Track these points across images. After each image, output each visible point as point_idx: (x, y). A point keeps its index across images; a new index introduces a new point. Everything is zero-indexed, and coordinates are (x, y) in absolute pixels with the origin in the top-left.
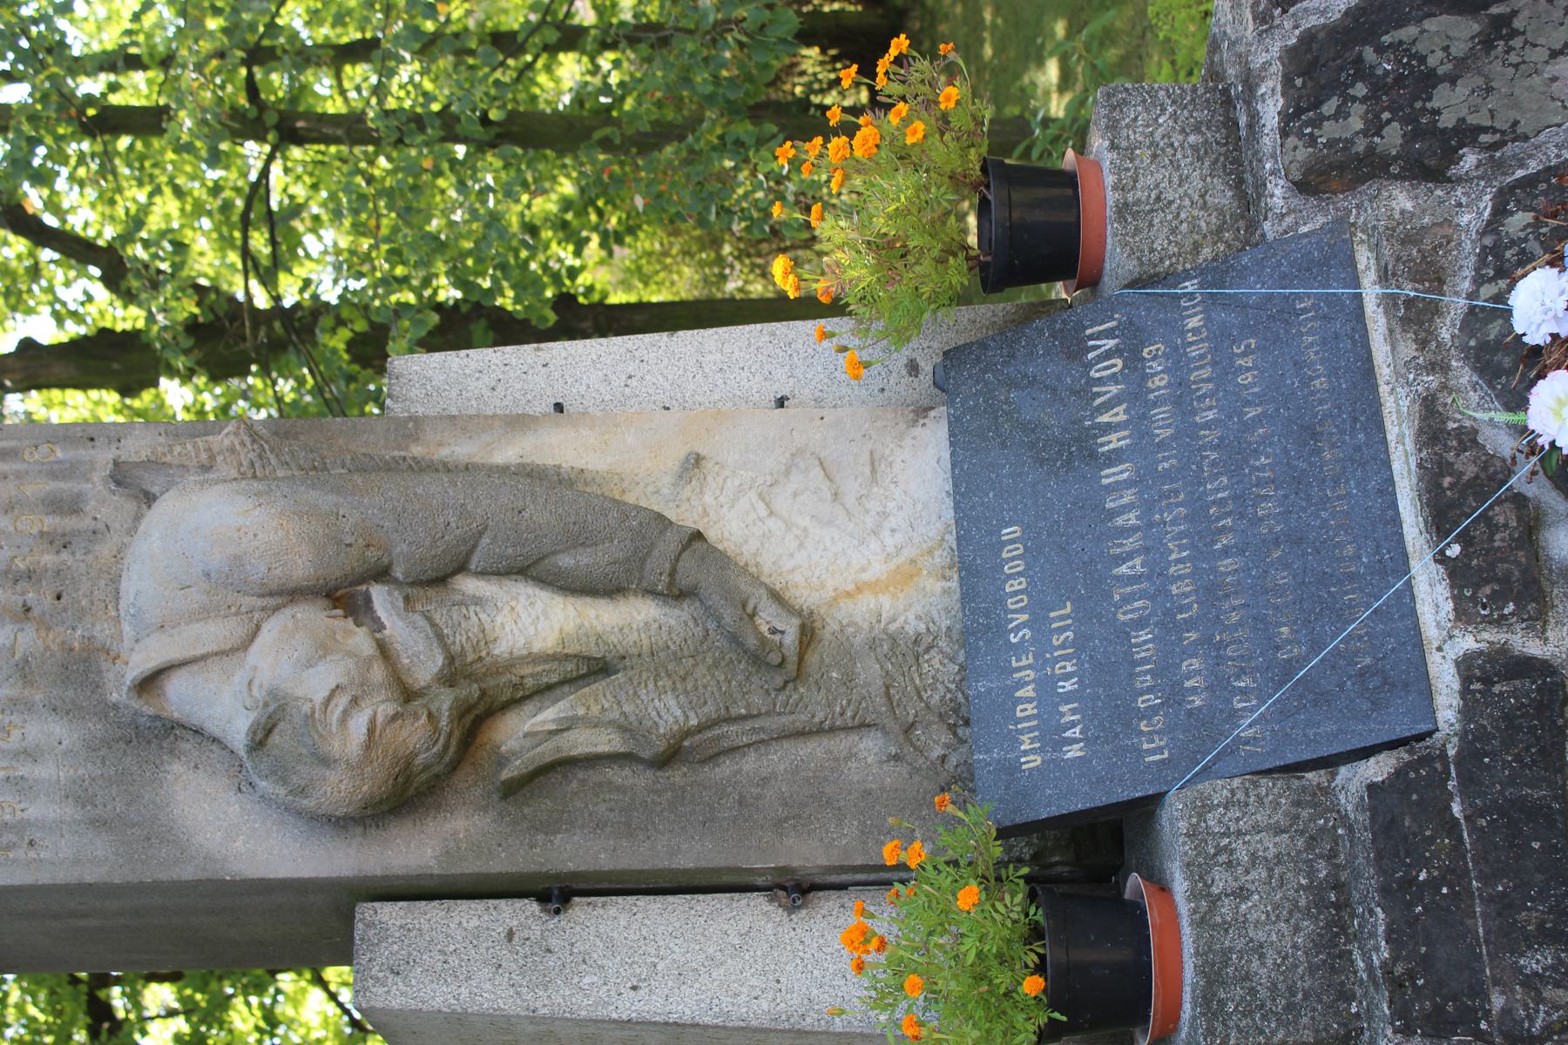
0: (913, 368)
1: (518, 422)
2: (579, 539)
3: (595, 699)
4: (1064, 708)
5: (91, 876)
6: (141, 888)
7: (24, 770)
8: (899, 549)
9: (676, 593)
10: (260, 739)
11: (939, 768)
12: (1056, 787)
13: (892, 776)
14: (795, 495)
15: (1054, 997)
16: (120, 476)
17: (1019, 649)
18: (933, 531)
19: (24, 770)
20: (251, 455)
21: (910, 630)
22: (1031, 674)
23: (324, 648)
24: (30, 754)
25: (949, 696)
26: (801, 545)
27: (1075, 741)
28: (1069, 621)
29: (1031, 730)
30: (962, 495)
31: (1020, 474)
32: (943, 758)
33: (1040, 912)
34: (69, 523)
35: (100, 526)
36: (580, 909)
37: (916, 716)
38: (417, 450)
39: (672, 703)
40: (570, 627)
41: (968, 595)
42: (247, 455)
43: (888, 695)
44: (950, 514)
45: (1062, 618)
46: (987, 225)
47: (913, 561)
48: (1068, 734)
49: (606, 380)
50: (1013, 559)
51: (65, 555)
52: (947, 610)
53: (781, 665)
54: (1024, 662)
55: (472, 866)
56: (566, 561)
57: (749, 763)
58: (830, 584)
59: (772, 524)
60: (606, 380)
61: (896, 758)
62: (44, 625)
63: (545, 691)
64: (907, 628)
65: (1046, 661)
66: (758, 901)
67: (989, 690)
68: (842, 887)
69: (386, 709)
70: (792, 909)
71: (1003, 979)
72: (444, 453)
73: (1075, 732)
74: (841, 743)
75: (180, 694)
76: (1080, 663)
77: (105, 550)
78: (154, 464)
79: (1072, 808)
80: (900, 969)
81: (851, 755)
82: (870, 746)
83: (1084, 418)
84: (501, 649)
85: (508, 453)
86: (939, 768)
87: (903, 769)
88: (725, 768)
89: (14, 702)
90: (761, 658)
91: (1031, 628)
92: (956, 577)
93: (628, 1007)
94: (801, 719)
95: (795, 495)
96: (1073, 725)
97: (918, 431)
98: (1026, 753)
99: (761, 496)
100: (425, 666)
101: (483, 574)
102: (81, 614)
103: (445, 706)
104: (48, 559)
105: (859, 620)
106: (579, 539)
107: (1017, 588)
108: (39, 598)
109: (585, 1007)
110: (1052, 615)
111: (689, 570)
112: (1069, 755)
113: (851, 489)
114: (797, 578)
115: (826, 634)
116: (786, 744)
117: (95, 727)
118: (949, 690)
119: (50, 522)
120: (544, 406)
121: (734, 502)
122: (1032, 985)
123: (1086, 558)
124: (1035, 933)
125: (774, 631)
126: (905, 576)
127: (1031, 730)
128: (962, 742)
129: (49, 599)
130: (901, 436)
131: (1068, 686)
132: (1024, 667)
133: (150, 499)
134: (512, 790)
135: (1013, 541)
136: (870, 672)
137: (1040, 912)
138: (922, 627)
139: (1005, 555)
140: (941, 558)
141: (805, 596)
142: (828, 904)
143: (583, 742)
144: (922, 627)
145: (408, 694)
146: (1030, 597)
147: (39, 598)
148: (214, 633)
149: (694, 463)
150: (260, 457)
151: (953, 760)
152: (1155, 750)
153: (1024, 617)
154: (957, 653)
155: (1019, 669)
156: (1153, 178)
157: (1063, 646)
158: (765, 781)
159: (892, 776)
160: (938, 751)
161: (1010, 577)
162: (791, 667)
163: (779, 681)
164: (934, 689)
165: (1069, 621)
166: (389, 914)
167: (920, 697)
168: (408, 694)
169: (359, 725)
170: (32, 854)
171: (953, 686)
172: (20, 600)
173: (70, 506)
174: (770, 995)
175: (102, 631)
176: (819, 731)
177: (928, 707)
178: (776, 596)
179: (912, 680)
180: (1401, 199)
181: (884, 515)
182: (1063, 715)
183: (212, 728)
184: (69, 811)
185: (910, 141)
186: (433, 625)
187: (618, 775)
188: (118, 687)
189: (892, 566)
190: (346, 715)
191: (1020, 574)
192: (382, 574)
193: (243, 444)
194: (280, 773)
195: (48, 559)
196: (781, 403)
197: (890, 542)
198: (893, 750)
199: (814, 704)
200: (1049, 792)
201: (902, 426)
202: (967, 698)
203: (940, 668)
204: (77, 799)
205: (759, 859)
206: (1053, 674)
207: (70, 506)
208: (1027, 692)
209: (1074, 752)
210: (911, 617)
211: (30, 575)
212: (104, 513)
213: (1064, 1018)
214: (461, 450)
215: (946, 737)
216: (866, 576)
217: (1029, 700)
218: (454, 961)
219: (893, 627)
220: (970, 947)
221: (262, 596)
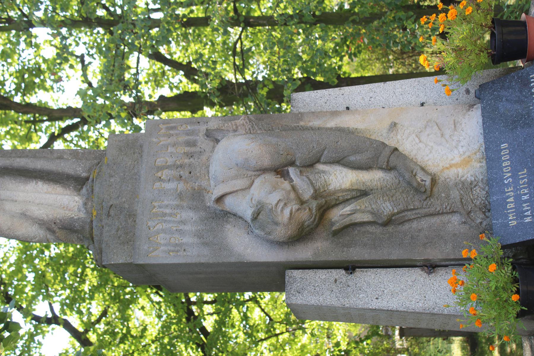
0: (468, 92)
1: (335, 113)
2: (357, 151)
3: (363, 203)
4: (524, 205)
5: (203, 260)
6: (218, 265)
7: (181, 227)
8: (464, 153)
9: (389, 168)
10: (255, 217)
11: (480, 226)
12: (522, 232)
13: (463, 229)
14: (428, 135)
15: (522, 302)
16: (208, 134)
17: (508, 185)
18: (476, 147)
19: (181, 227)
20: (249, 126)
21: (469, 180)
22: (512, 194)
23: (275, 188)
24: (183, 222)
25: (482, 202)
26: (431, 152)
27: (528, 216)
28: (526, 176)
29: (512, 212)
30: (487, 133)
31: (507, 126)
32: (481, 223)
33: (517, 273)
34: (193, 149)
35: (202, 150)
36: (359, 273)
37: (471, 208)
38: (302, 123)
39: (388, 205)
40: (354, 180)
41: (489, 168)
42: (248, 126)
43: (461, 201)
44: (482, 140)
45: (523, 174)
46: (494, 41)
47: (469, 157)
48: (526, 214)
49: (363, 98)
50: (505, 155)
51: (192, 160)
52: (482, 173)
53: (425, 192)
54: (510, 190)
55: (323, 258)
56: (352, 158)
57: (415, 224)
58: (441, 165)
59: (421, 145)
60: (363, 98)
61: (465, 223)
62: (186, 182)
63: (346, 201)
64: (468, 179)
65: (517, 189)
66: (418, 270)
67: (497, 199)
68: (446, 266)
69: (295, 207)
70: (429, 273)
71: (505, 296)
72: (311, 124)
73: (529, 213)
74: (445, 218)
75: (230, 203)
76: (530, 190)
77: (204, 158)
78: (219, 130)
79: (528, 239)
80: (468, 292)
81: (449, 222)
82: (455, 219)
83: (530, 106)
84: (331, 187)
85: (332, 124)
86: (480, 226)
87: (467, 227)
88: (407, 226)
89: (178, 206)
90: (418, 190)
91: (512, 178)
92: (484, 162)
93: (375, 304)
94: (432, 210)
95: (428, 135)
96: (528, 210)
97: (470, 113)
98: (511, 220)
99: (417, 136)
100: (307, 193)
101: (325, 163)
103: (314, 206)
104: (187, 161)
105: (451, 177)
106: (357, 151)
107: (507, 164)
109: (360, 304)
110: (520, 173)
111: (394, 161)
112: (526, 221)
113: (447, 133)
114: (430, 163)
115: (440, 181)
116: (427, 218)
117: (203, 214)
118: (482, 200)
119: (187, 149)
120: (342, 108)
121: (408, 138)
122: (515, 298)
123: (531, 154)
124: (515, 281)
125: (422, 181)
126: (467, 162)
127: (512, 212)
128: (488, 217)
129: (187, 174)
130: (464, 115)
131: (526, 197)
132: (510, 192)
133: (217, 141)
134: (336, 233)
135: (505, 149)
136: (455, 194)
137: (517, 273)
138: (473, 179)
139: (502, 154)
140: (479, 155)
141: (432, 169)
142: (441, 272)
143: (359, 218)
144: (473, 179)
145: (302, 203)
146: (511, 167)
147: (185, 173)
148: (240, 183)
149: (394, 125)
150: (252, 127)
151: (484, 223)
153: (510, 174)
154: (485, 187)
155: (508, 192)
157: (524, 184)
158: (420, 230)
159: (463, 229)
160: (479, 221)
161: (504, 161)
162: (428, 192)
163: (424, 197)
164: (478, 200)
165: (526, 176)
166: (297, 273)
167: (473, 202)
168: (302, 203)
169: (287, 212)
170: (185, 253)
171: (484, 199)
172: (179, 174)
173: (193, 144)
174: (422, 302)
175: (204, 184)
176: (438, 214)
177: (475, 205)
178: (423, 169)
179: (470, 196)
181: (459, 141)
182: (524, 207)
183: (240, 214)
184: (196, 240)
185: (467, 13)
186: (310, 180)
187: (371, 229)
188: (210, 200)
189: (462, 158)
190: (282, 211)
191: (508, 160)
192: (292, 164)
193: (246, 123)
194: (262, 228)
195: (187, 161)
196: (422, 105)
197: (461, 150)
198: (464, 220)
199: (436, 205)
200: (519, 233)
201: (465, 111)
202: (489, 203)
203: (479, 193)
204: (198, 236)
205: (418, 256)
206: (520, 193)
207: (193, 144)
208: (511, 200)
209: (528, 220)
210: (469, 175)
211: (181, 166)
213: (526, 309)
214: (316, 123)
215: (482, 216)
216: (453, 162)
217: (512, 202)
218: (317, 288)
219: (463, 179)
220: (493, 285)
221: (255, 171)
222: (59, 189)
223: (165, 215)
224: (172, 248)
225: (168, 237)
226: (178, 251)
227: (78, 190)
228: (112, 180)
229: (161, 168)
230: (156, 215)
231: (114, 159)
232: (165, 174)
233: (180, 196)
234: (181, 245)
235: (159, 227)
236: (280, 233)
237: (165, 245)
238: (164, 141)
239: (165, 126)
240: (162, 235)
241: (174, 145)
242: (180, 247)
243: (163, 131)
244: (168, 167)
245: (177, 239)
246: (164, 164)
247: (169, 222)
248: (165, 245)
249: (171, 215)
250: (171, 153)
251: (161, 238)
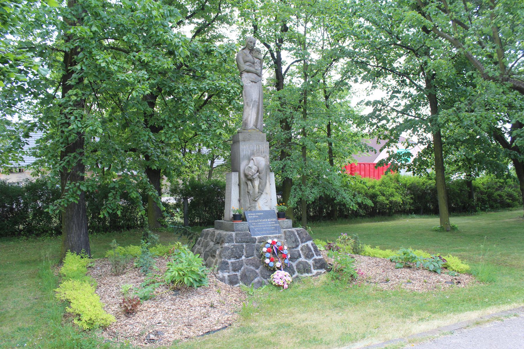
1: (269, 182)
10: (250, 167)
75: (252, 161)
82: (249, 205)
85: (267, 181)
93: (232, 189)
100: (254, 177)
106: (262, 186)
126: (260, 207)
134: (246, 183)
143: (249, 187)
148: (256, 163)
152: (250, 221)
156: (286, 223)
180: (283, 237)
214: (268, 178)
222: (255, 121)
227: (254, 125)
232: (258, 147)
236: (247, 172)
245: (245, 150)
251: (245, 147)
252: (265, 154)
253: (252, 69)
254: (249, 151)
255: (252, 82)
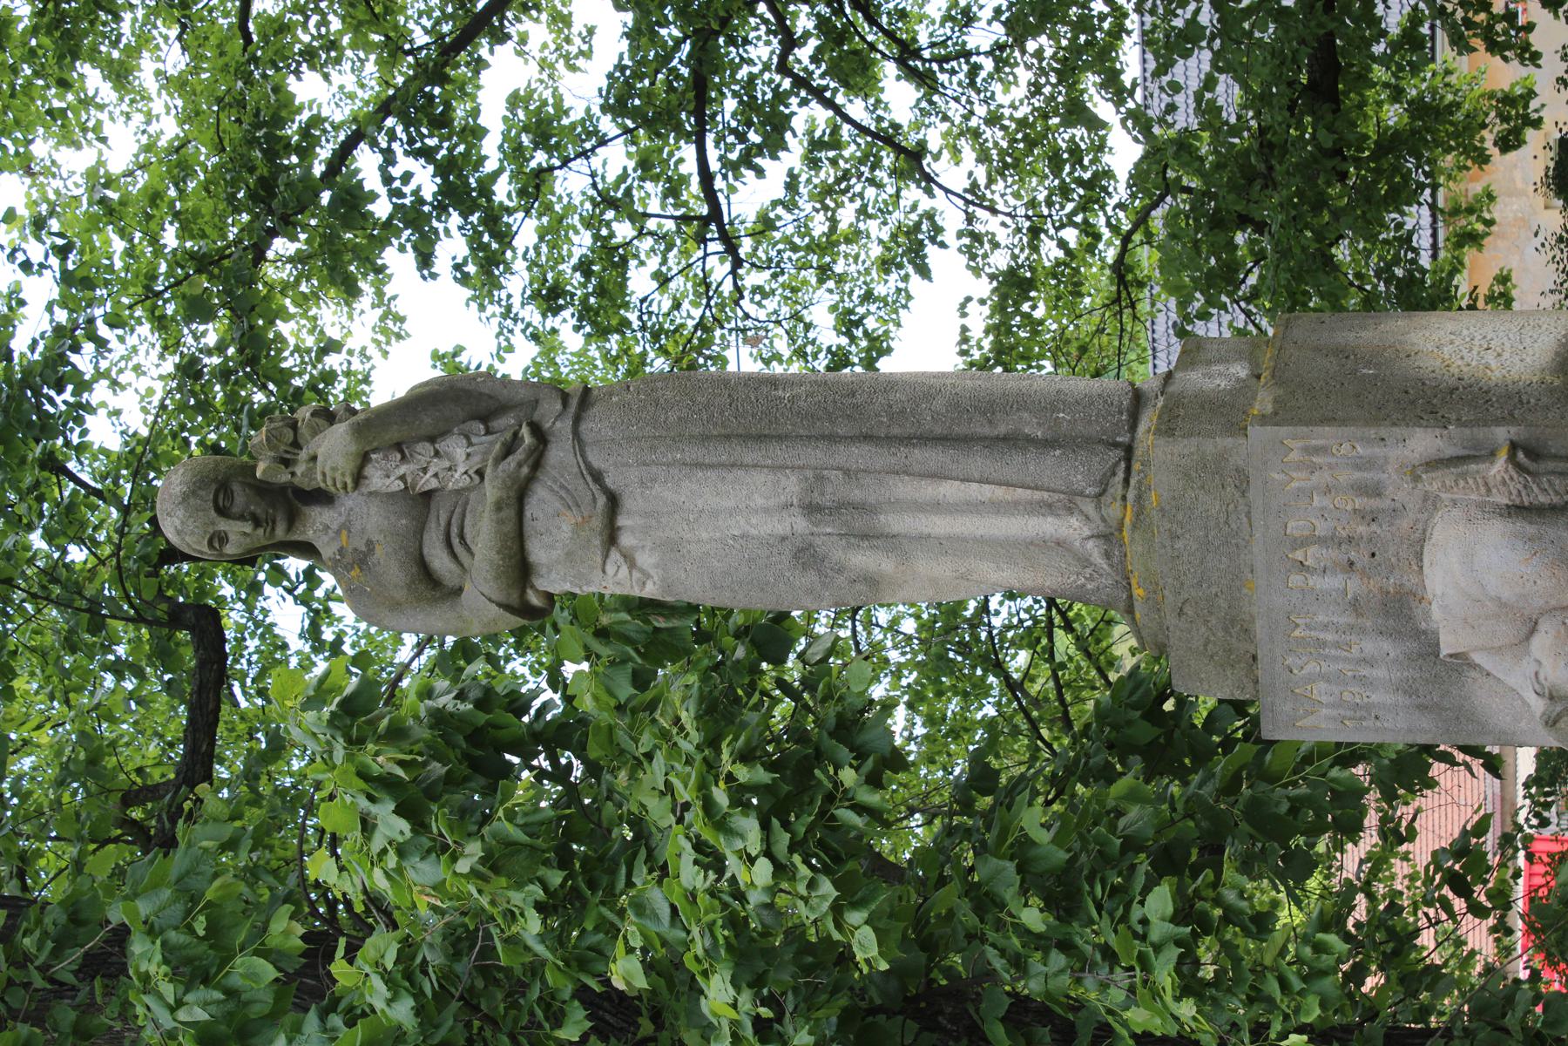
20: (1519, 486)
34: (1374, 503)
35: (1398, 505)
51: (1374, 527)
62: (1364, 574)
77: (1404, 524)
102: (1392, 568)
104: (1362, 529)
108: (1360, 556)
117: (1412, 645)
119: (1360, 502)
129: (1367, 558)
150: (1525, 487)
170: (1378, 724)
173: (1375, 491)
175: (1411, 581)
184: (1401, 699)
193: (1512, 478)
204: (1405, 692)
212: (1399, 496)
223: (1322, 644)
224: (1349, 713)
225: (1336, 689)
226: (1362, 718)
228: (1179, 545)
229: (1303, 543)
230: (1301, 642)
231: (1174, 498)
232: (1312, 555)
233: (1355, 606)
234: (1368, 707)
235: (1312, 667)
237: (1332, 706)
238: (1299, 480)
239: (1300, 444)
240: (1323, 685)
241: (1328, 490)
242: (1363, 711)
243: (1294, 456)
244: (1322, 541)
246: (1306, 533)
247: (1336, 659)
248: (1332, 706)
249: (1337, 645)
250: (1323, 509)
251: (1320, 690)
252: (1389, 476)
253: (484, 534)
254: (1370, 646)
255: (611, 537)
